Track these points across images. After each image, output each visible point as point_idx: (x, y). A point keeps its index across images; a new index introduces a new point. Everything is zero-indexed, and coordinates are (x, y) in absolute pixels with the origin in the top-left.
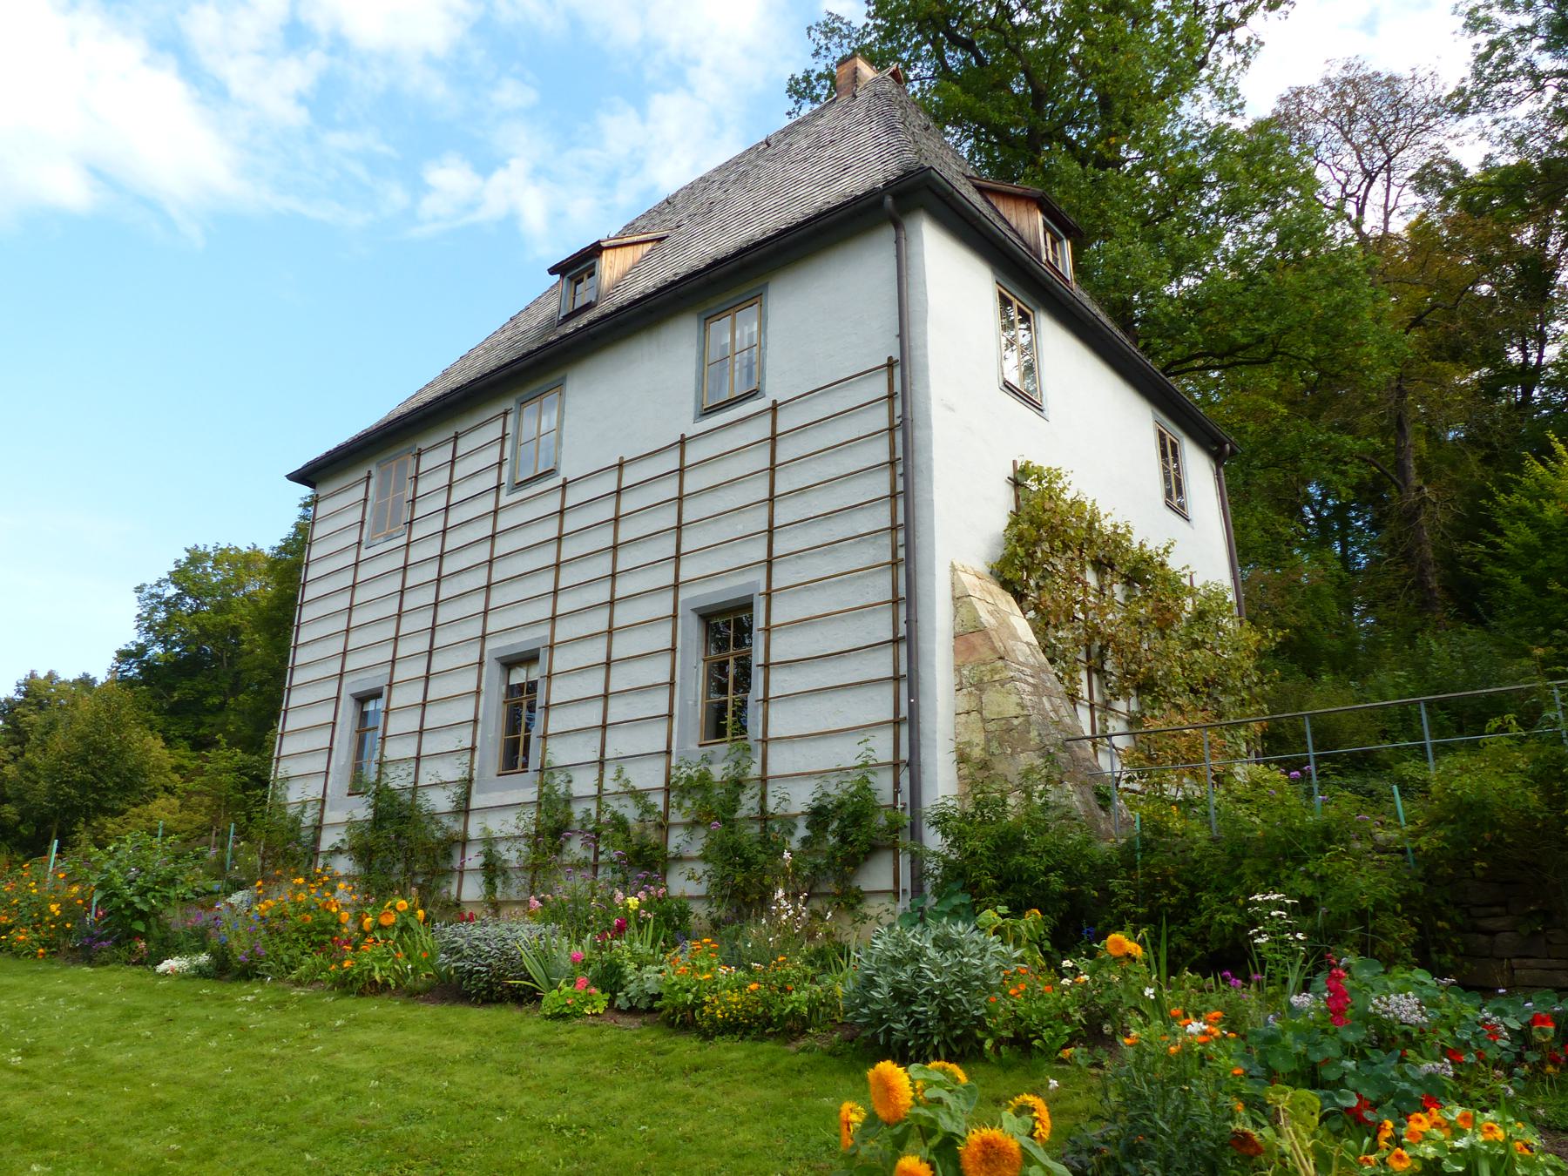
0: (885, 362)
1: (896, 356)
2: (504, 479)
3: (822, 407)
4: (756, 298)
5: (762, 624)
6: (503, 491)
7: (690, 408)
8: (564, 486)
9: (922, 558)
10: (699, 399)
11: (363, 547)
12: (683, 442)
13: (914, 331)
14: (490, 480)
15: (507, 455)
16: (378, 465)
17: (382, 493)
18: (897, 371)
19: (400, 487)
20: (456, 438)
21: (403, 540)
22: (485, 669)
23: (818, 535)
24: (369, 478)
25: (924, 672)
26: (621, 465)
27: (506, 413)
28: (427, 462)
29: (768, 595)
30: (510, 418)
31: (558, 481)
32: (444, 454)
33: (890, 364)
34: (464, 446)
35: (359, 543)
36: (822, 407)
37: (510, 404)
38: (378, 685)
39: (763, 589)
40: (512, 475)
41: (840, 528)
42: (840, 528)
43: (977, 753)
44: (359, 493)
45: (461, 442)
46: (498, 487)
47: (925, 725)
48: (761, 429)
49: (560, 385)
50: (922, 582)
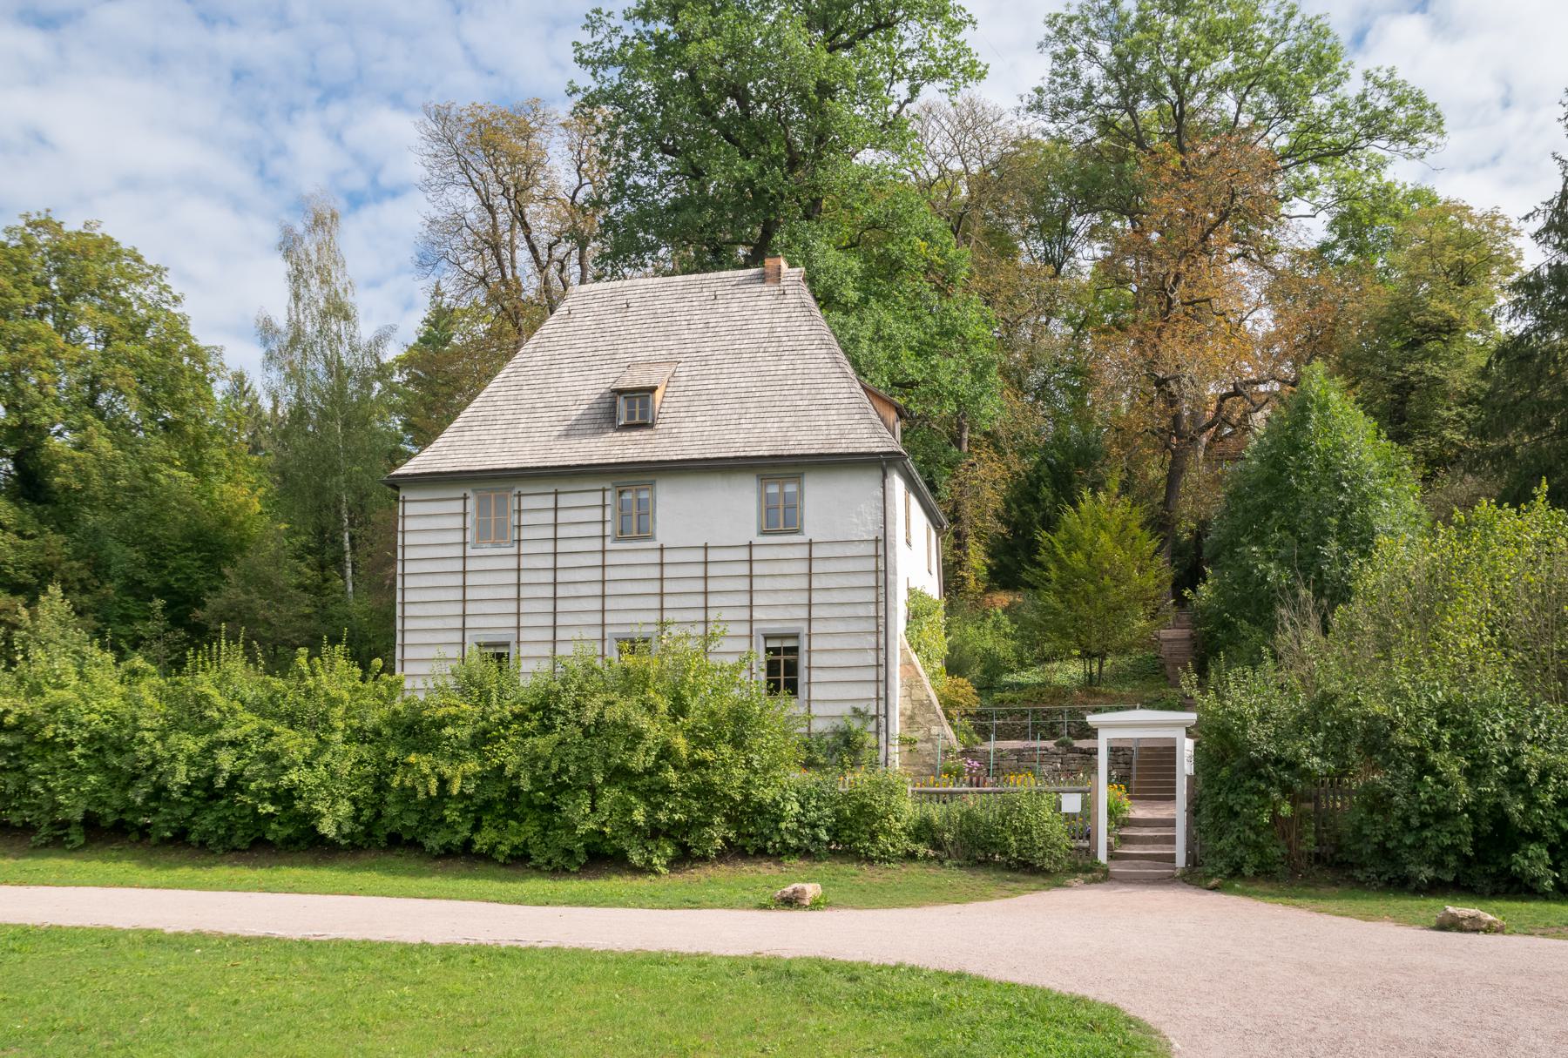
0: (873, 538)
1: (881, 537)
2: (608, 532)
3: (838, 551)
4: (797, 478)
5: (806, 648)
6: (608, 541)
7: (754, 528)
8: (662, 549)
9: (891, 631)
10: (760, 525)
11: (468, 547)
12: (750, 546)
13: (889, 527)
14: (596, 530)
15: (608, 517)
16: (474, 490)
17: (481, 510)
18: (881, 545)
19: (501, 510)
20: (556, 493)
21: (514, 550)
22: (606, 644)
23: (837, 612)
24: (465, 498)
25: (890, 680)
26: (706, 548)
27: (604, 490)
28: (527, 503)
29: (809, 636)
30: (608, 495)
31: (656, 544)
32: (549, 502)
33: (877, 540)
34: (564, 501)
35: (465, 543)
36: (838, 551)
37: (608, 485)
38: (504, 639)
39: (806, 631)
40: (614, 531)
41: (848, 611)
42: (848, 611)
43: (908, 713)
44: (457, 506)
45: (560, 497)
46: (603, 537)
47: (891, 701)
48: (803, 552)
49: (653, 484)
50: (890, 642)
